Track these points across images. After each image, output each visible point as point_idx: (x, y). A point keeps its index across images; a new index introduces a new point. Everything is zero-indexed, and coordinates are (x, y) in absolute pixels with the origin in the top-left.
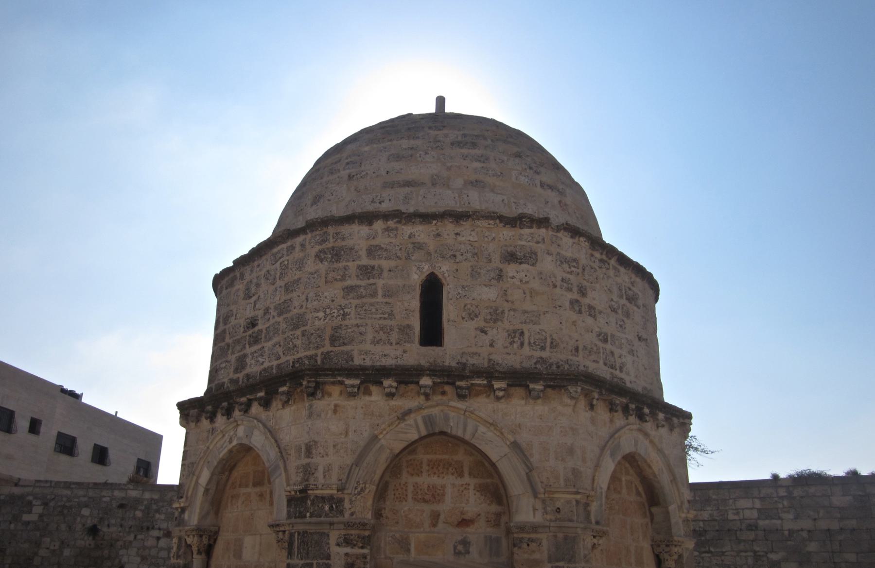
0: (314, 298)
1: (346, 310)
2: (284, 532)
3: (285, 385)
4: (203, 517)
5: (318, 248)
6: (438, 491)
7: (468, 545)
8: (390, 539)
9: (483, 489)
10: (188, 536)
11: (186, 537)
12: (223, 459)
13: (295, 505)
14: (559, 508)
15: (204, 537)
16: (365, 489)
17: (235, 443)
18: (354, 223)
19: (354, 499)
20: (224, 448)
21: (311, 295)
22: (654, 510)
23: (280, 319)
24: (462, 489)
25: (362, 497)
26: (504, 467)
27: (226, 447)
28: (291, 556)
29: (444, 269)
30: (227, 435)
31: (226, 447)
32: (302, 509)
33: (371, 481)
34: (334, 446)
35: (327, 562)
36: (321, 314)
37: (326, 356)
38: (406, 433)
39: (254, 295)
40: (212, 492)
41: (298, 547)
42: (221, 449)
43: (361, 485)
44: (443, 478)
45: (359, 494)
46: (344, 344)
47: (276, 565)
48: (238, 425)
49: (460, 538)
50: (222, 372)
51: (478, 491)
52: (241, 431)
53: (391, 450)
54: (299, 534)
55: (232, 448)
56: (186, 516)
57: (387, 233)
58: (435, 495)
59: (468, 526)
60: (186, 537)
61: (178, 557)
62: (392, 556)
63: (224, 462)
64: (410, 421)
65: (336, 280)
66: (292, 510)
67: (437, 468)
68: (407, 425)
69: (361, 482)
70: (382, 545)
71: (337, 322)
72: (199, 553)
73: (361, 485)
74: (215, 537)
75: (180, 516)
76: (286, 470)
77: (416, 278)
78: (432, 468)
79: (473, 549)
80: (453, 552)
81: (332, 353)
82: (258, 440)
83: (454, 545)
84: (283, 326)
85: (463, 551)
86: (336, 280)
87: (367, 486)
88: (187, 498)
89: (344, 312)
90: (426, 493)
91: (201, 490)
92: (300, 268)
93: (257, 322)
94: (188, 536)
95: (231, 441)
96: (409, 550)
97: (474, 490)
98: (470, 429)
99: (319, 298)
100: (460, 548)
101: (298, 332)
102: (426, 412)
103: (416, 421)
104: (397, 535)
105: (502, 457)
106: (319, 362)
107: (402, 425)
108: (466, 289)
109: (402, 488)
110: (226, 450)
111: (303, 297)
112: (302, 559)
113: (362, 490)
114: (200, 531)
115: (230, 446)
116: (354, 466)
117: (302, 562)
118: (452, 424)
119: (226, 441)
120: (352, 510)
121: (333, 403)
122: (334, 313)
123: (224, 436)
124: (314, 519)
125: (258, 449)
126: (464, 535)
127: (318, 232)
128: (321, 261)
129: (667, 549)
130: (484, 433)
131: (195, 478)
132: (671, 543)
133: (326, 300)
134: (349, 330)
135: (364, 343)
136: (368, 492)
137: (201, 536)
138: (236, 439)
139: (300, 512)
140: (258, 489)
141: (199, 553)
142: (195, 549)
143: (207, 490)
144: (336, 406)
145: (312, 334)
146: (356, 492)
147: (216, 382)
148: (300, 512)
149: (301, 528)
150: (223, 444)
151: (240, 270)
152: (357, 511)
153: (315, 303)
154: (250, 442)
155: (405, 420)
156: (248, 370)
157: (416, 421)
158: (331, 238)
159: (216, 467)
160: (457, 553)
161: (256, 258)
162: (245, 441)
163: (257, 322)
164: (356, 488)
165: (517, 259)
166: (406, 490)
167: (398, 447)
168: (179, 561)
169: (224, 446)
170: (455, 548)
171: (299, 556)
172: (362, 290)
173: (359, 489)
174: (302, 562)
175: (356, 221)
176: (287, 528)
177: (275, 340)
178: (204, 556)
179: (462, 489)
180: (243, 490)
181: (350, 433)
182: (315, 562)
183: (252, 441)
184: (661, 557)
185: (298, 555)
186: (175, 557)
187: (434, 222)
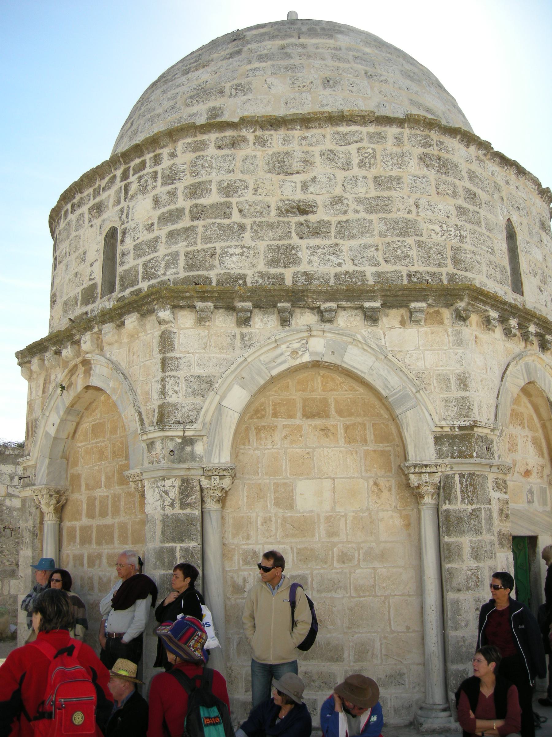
0: (427, 207)
1: (462, 232)
3: (425, 300)
5: (421, 150)
13: (450, 444)
18: (455, 137)
20: (281, 363)
21: (422, 202)
23: (373, 217)
27: (284, 362)
28: (449, 500)
32: (464, 449)
34: (481, 381)
35: (488, 506)
36: (437, 228)
37: (452, 277)
39: (298, 173)
41: (462, 491)
42: (274, 364)
46: (466, 269)
47: (370, 514)
50: (234, 258)
54: (462, 475)
56: (199, 448)
57: (478, 162)
61: (183, 506)
65: (448, 194)
66: (444, 449)
71: (455, 242)
75: (183, 449)
77: (502, 221)
81: (457, 276)
84: (378, 227)
86: (448, 194)
89: (460, 233)
92: (399, 165)
93: (315, 209)
99: (433, 209)
101: (410, 240)
106: (445, 282)
111: (411, 201)
112: (472, 504)
117: (470, 508)
122: (451, 231)
123: (277, 346)
124: (479, 460)
127: (418, 132)
128: (428, 166)
131: (218, 398)
133: (440, 213)
134: (468, 256)
135: (481, 273)
139: (460, 452)
140: (317, 422)
145: (431, 248)
147: (218, 270)
148: (460, 452)
149: (466, 469)
151: (254, 132)
153: (429, 213)
154: (343, 361)
156: (303, 267)
158: (435, 145)
161: (299, 128)
163: (315, 209)
168: (188, 511)
169: (279, 361)
171: (466, 500)
172: (471, 215)
174: (470, 508)
175: (458, 137)
177: (365, 240)
180: (281, 422)
182: (482, 507)
185: (463, 499)
186: (177, 505)
187: (506, 168)
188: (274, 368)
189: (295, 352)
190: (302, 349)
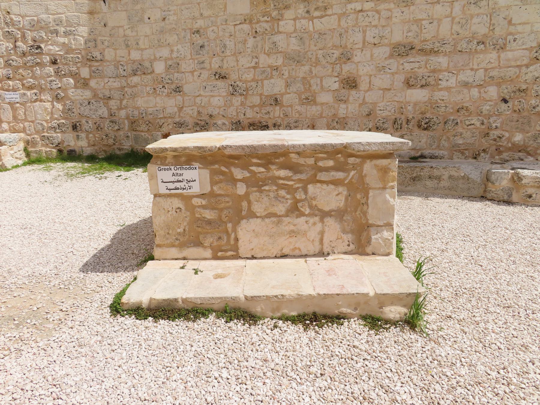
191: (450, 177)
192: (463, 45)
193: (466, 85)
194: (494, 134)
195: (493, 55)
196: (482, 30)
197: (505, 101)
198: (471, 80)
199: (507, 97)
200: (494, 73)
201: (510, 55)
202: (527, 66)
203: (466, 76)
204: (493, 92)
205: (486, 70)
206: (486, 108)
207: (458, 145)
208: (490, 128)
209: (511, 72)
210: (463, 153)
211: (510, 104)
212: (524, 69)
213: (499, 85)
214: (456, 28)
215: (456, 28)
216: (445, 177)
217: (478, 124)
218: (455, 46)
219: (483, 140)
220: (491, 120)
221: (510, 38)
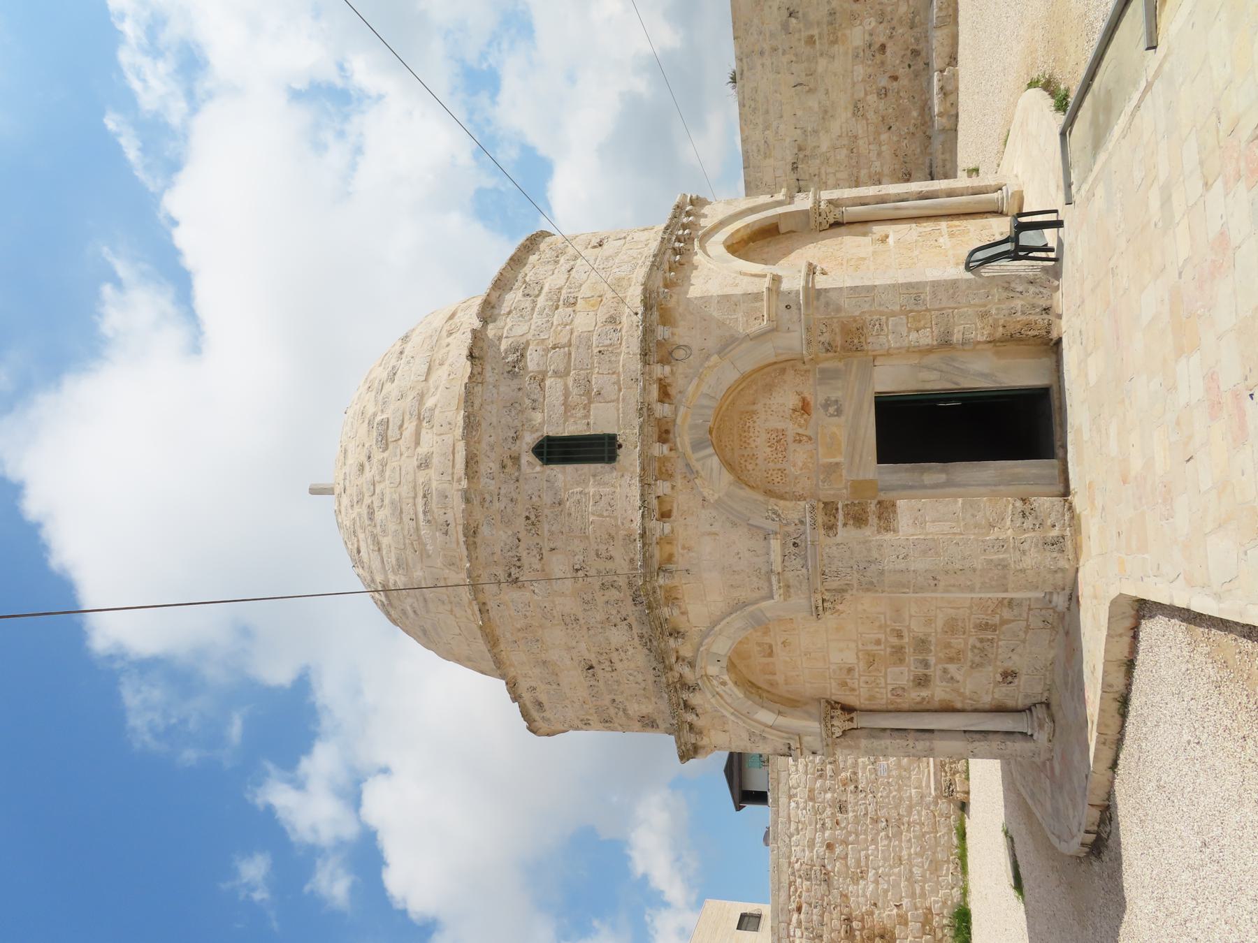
2: (823, 600)
4: (810, 716)
6: (774, 436)
7: (829, 402)
8: (826, 484)
9: (769, 388)
10: (833, 733)
11: (834, 737)
12: (745, 693)
14: (786, 307)
15: (832, 714)
16: (774, 509)
17: (726, 678)
19: (785, 522)
20: (732, 691)
22: (783, 229)
24: (770, 412)
25: (782, 513)
26: (747, 365)
27: (730, 689)
29: (530, 439)
30: (718, 690)
31: (730, 689)
33: (765, 504)
38: (712, 469)
40: (782, 708)
42: (733, 696)
43: (770, 514)
44: (759, 432)
45: (779, 516)
48: (706, 675)
49: (822, 410)
51: (771, 395)
52: (713, 670)
53: (731, 484)
55: (732, 682)
58: (778, 440)
59: (808, 404)
60: (834, 737)
62: (844, 481)
63: (747, 692)
64: (697, 466)
67: (749, 439)
68: (703, 470)
69: (767, 514)
70: (832, 492)
72: (851, 720)
73: (770, 514)
74: (833, 703)
76: (756, 602)
78: (749, 444)
79: (834, 396)
80: (837, 418)
82: (722, 646)
83: (829, 417)
85: (836, 407)
87: (770, 508)
88: (790, 738)
90: (776, 449)
91: (782, 721)
94: (833, 733)
95: (724, 684)
96: (837, 464)
97: (770, 399)
98: (705, 402)
100: (831, 410)
102: (689, 450)
103: (698, 460)
104: (822, 477)
105: (735, 367)
107: (702, 473)
108: (551, 413)
109: (771, 475)
110: (736, 690)
113: (774, 513)
114: (827, 720)
115: (730, 684)
116: (751, 522)
118: (701, 421)
119: (725, 691)
120: (797, 522)
121: (680, 551)
123: (718, 693)
125: (733, 644)
126: (819, 406)
129: (824, 215)
130: (710, 386)
131: (767, 729)
132: (817, 210)
136: (777, 506)
137: (832, 717)
138: (722, 677)
141: (851, 720)
142: (848, 725)
143: (780, 713)
144: (683, 548)
146: (778, 519)
150: (728, 694)
152: (798, 517)
154: (725, 655)
155: (697, 472)
157: (698, 460)
159: (754, 702)
160: (839, 412)
162: (724, 663)
164: (773, 520)
165: (517, 360)
166: (773, 470)
167: (727, 477)
170: (832, 415)
173: (774, 516)
176: (819, 597)
178: (854, 715)
179: (770, 412)
181: (714, 530)
183: (723, 653)
184: (832, 221)
188: (736, 695)
189: (724, 684)
190: (718, 679)
191: (943, 154)
192: (853, 162)
193: (879, 154)
194: (912, 129)
195: (861, 142)
196: (844, 152)
197: (890, 128)
198: (876, 152)
199: (888, 127)
200: (871, 138)
201: (860, 132)
202: (867, 119)
203: (873, 156)
204: (884, 137)
205: (869, 144)
206: (895, 139)
207: (922, 152)
208: (908, 133)
209: (871, 128)
210: (928, 146)
211: (892, 124)
212: (869, 122)
213: (879, 134)
214: (842, 168)
215: (842, 168)
216: (943, 156)
217: (906, 141)
218: (853, 167)
219: (917, 135)
220: (903, 133)
221: (850, 135)
